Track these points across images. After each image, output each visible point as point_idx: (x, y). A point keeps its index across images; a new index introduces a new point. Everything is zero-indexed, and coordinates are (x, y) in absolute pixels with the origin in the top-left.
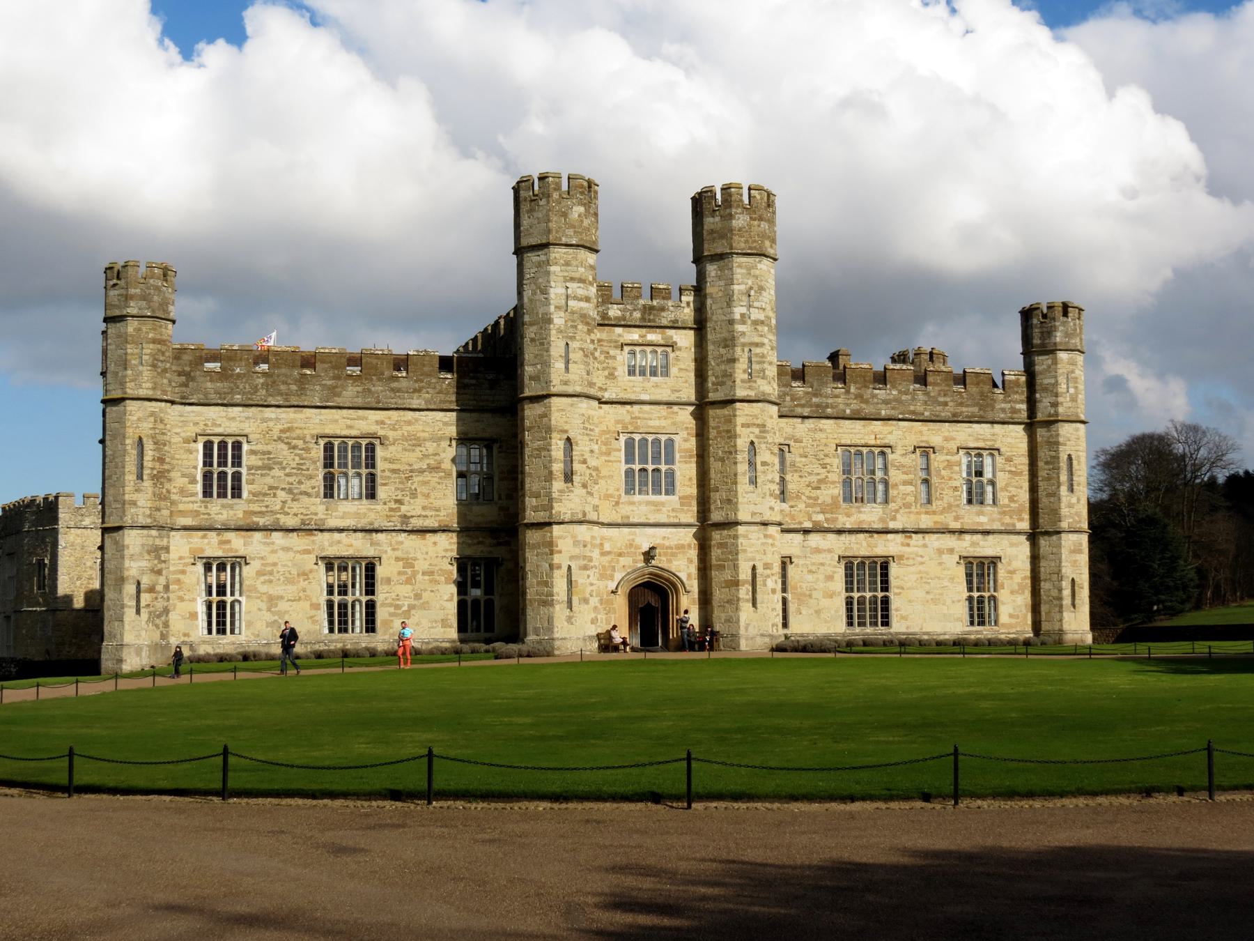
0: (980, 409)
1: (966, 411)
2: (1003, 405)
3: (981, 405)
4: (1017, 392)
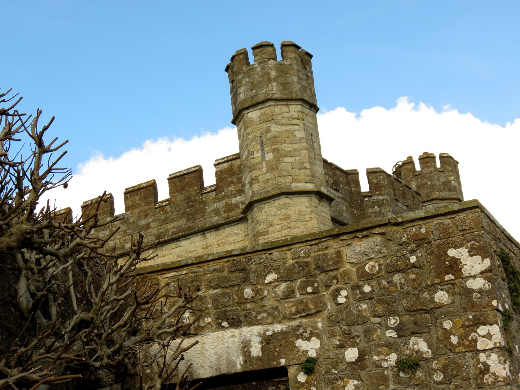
0: (188, 220)
1: (172, 227)
2: (216, 205)
3: (189, 214)
4: (232, 182)
